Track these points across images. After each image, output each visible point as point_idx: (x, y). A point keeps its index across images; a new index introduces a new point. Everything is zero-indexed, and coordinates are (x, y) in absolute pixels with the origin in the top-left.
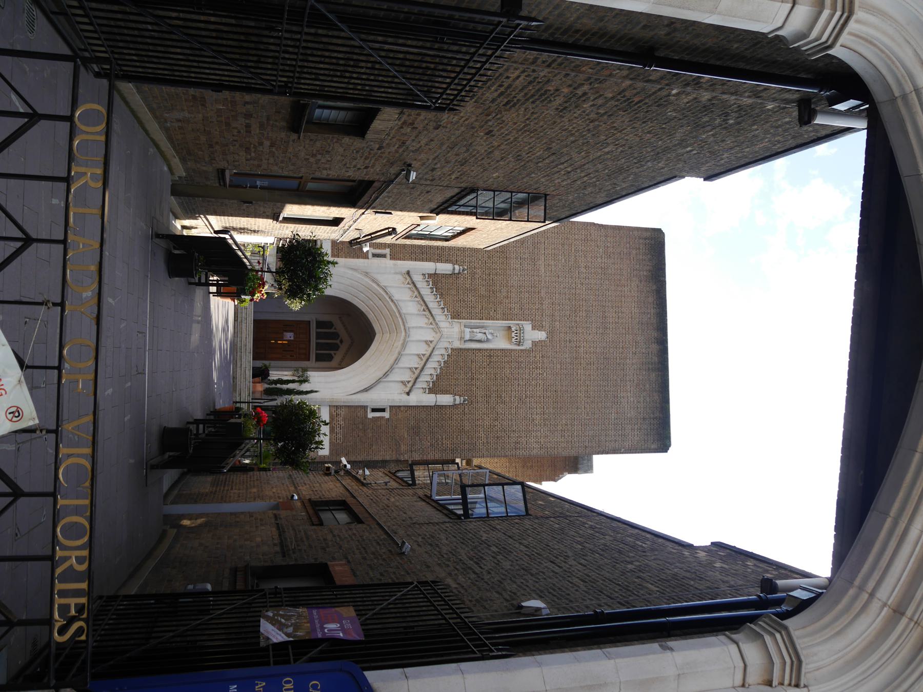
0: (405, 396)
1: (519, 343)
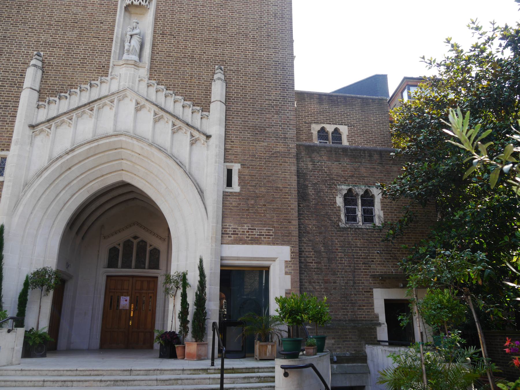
0: (211, 140)
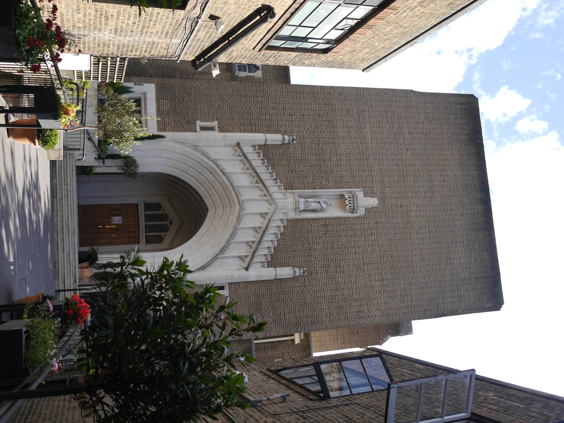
0: (244, 272)
1: (353, 211)
